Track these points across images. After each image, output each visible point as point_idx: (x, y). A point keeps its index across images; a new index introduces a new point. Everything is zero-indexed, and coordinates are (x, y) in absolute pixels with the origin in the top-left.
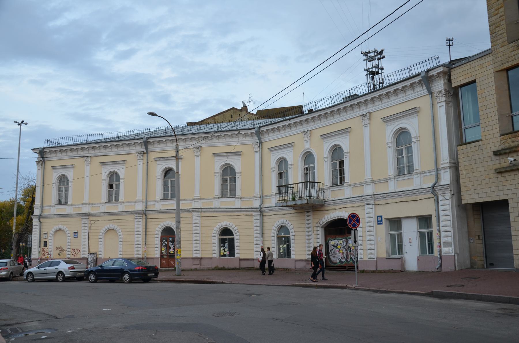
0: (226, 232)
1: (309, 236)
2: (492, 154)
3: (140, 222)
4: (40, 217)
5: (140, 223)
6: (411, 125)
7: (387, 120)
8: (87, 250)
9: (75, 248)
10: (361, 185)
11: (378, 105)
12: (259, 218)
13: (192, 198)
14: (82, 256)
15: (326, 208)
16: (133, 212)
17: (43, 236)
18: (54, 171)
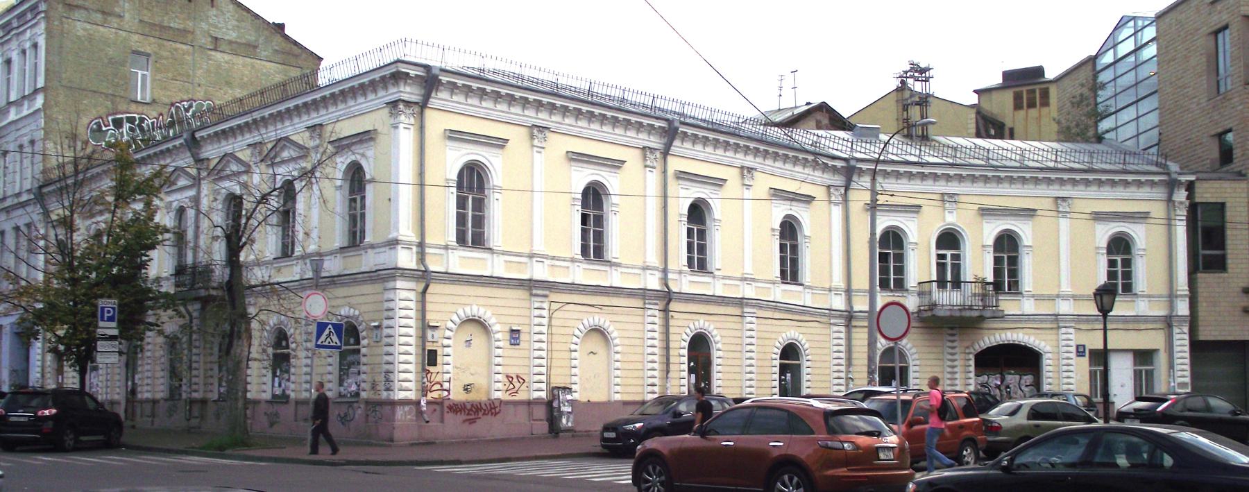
0: (790, 352)
1: (953, 367)
2: (1239, 290)
5: (656, 320)
6: (1137, 232)
7: (1099, 217)
8: (543, 378)
9: (513, 371)
10: (1052, 298)
11: (1093, 191)
12: (843, 329)
13: (739, 275)
14: (536, 395)
15: (985, 326)
16: (643, 294)
18: (450, 143)
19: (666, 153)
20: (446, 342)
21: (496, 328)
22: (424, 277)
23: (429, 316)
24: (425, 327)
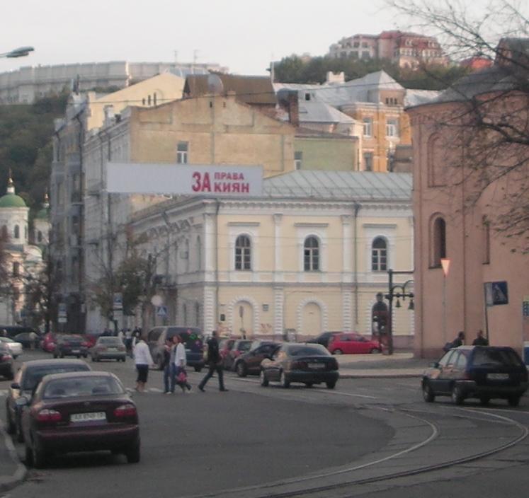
3: (348, 296)
4: (217, 285)
14: (277, 333)
16: (341, 285)
17: (221, 308)
19: (356, 216)
20: (229, 311)
21: (255, 304)
22: (217, 285)
23: (220, 300)
24: (218, 306)
